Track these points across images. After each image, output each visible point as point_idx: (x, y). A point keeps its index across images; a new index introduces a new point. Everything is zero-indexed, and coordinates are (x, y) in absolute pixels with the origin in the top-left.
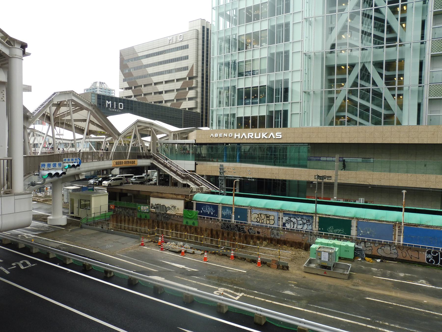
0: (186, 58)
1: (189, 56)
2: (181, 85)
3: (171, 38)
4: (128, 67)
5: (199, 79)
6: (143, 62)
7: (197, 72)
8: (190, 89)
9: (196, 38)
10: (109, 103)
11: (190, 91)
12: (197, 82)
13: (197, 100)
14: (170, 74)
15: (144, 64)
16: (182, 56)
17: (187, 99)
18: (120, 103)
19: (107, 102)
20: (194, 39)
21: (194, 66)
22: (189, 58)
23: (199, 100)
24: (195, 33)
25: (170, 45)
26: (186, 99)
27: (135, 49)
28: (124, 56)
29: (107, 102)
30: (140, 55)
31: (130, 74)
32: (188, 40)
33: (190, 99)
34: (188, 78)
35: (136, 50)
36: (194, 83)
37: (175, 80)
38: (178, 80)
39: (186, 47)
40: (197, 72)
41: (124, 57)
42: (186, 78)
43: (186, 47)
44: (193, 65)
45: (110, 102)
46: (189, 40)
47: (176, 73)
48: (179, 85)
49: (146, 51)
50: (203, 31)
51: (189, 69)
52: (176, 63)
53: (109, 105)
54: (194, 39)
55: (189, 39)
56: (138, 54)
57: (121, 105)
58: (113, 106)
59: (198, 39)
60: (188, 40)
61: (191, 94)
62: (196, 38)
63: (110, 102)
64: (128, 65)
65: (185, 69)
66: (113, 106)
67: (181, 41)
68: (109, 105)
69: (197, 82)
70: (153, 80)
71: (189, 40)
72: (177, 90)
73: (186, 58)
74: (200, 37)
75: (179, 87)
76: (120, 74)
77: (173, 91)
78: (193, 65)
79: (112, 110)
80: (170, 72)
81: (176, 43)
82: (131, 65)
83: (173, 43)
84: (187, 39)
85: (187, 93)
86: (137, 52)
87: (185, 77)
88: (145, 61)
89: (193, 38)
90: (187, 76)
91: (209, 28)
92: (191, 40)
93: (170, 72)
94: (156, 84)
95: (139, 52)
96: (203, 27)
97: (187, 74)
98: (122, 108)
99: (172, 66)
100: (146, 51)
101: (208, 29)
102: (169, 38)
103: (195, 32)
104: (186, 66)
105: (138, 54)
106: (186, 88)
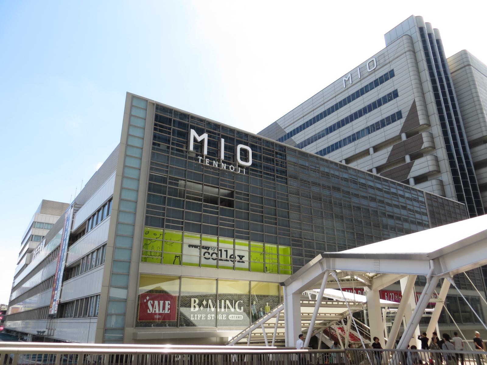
2: (387, 155)
3: (350, 75)
5: (437, 130)
6: (295, 140)
7: (427, 116)
9: (409, 51)
10: (199, 139)
11: (417, 162)
13: (440, 178)
14: (356, 142)
18: (240, 146)
19: (193, 133)
20: (405, 53)
21: (417, 104)
22: (399, 94)
23: (447, 177)
24: (405, 41)
25: (348, 89)
27: (279, 124)
29: (193, 133)
30: (288, 131)
32: (389, 62)
33: (419, 179)
35: (281, 126)
36: (425, 139)
37: (371, 151)
38: (376, 149)
40: (427, 116)
42: (399, 137)
44: (414, 103)
45: (205, 136)
46: (393, 60)
47: (370, 135)
48: (382, 157)
51: (405, 115)
53: (199, 145)
54: (405, 53)
55: (390, 59)
56: (285, 130)
57: (244, 153)
58: (214, 153)
59: (414, 52)
60: (389, 62)
62: (409, 51)
63: (205, 136)
66: (214, 153)
67: (375, 71)
68: (199, 145)
71: (393, 60)
74: (419, 46)
75: (384, 161)
78: (414, 103)
79: (211, 163)
80: (354, 138)
83: (354, 83)
84: (388, 61)
85: (410, 166)
86: (283, 128)
87: (397, 133)
89: (403, 51)
90: (402, 132)
93: (354, 138)
97: (400, 127)
98: (249, 164)
101: (430, 35)
102: (344, 78)
103: (405, 40)
106: (404, 159)
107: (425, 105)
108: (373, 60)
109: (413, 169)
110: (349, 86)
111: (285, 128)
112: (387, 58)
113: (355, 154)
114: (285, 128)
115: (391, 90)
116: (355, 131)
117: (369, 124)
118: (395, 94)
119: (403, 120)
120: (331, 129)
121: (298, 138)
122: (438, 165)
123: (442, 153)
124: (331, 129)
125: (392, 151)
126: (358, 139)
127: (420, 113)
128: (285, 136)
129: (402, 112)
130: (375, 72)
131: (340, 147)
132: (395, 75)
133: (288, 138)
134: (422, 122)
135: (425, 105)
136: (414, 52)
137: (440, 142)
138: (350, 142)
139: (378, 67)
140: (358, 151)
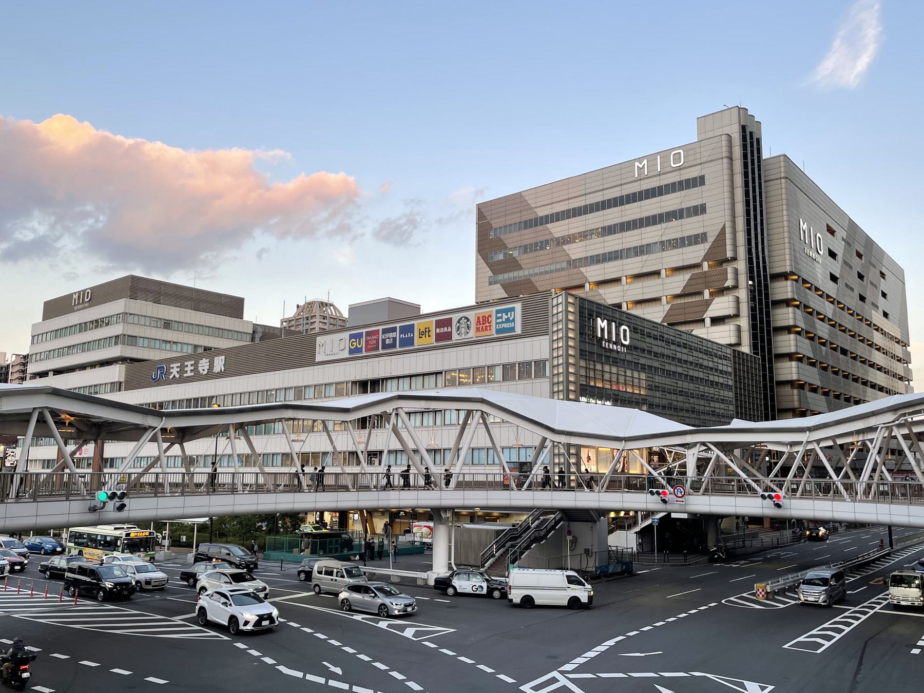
0: (700, 210)
1: (707, 206)
2: (683, 284)
4: (504, 246)
5: (742, 265)
6: (552, 231)
8: (722, 291)
9: (728, 157)
12: (736, 272)
14: (645, 257)
15: (556, 235)
16: (684, 206)
17: (708, 321)
20: (722, 158)
22: (708, 211)
23: (744, 322)
25: (640, 180)
26: (703, 321)
27: (526, 198)
28: (491, 219)
31: (512, 264)
32: (701, 164)
33: (716, 321)
34: (705, 265)
36: (730, 275)
39: (700, 181)
40: (735, 246)
41: (492, 222)
43: (700, 181)
44: (724, 227)
48: (678, 283)
49: (578, 197)
50: (744, 138)
51: (711, 239)
52: (664, 225)
54: (722, 158)
55: (703, 160)
56: (537, 210)
58: (610, 332)
59: (731, 158)
60: (701, 164)
61: (721, 306)
64: (506, 242)
67: (680, 169)
69: (736, 272)
70: (587, 275)
73: (700, 210)
75: (678, 291)
76: (477, 265)
78: (724, 227)
81: (660, 175)
82: (512, 240)
84: (698, 161)
85: (708, 304)
89: (719, 156)
90: (704, 260)
91: (755, 130)
92: (712, 163)
95: (538, 205)
96: (744, 128)
97: (703, 253)
99: (651, 234)
100: (578, 197)
101: (751, 133)
104: (700, 231)
105: (537, 210)
106: (700, 293)
107: (734, 233)
108: (680, 153)
109: (712, 307)
110: (642, 177)
111: (536, 207)
112: (698, 156)
113: (641, 272)
114: (536, 207)
115: (698, 202)
116: (645, 242)
117: (665, 238)
119: (707, 245)
120: (609, 230)
121: (558, 229)
122: (738, 308)
123: (743, 294)
124: (609, 230)
126: (647, 254)
127: (729, 242)
128: (536, 219)
129: (708, 235)
130: (680, 169)
131: (621, 258)
132: (706, 184)
133: (541, 224)
134: (729, 254)
135: (734, 233)
136: (731, 158)
137: (743, 280)
138: (636, 255)
139: (686, 165)
140: (645, 270)
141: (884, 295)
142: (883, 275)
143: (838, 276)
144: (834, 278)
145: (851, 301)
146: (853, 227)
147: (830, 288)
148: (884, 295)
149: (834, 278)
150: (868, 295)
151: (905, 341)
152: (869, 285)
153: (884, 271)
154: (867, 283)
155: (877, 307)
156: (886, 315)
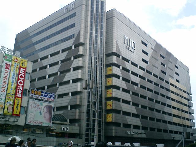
2: (66, 55)
7: (85, 38)
17: (72, 70)
30: (31, 35)
33: (75, 69)
38: (63, 51)
39: (74, 15)
40: (85, 38)
51: (75, 36)
65: (71, 37)
72: (62, 61)
73: (73, 26)
75: (63, 58)
77: (57, 63)
88: (34, 40)
94: (42, 59)
118: (73, 26)
125: (68, 53)
141: (177, 74)
142: (177, 67)
143: (148, 61)
144: (144, 61)
145: (157, 72)
146: (158, 47)
147: (144, 65)
148: (177, 74)
149: (144, 61)
150: (168, 72)
151: (189, 92)
152: (168, 68)
153: (177, 65)
154: (167, 67)
155: (173, 78)
156: (178, 81)
